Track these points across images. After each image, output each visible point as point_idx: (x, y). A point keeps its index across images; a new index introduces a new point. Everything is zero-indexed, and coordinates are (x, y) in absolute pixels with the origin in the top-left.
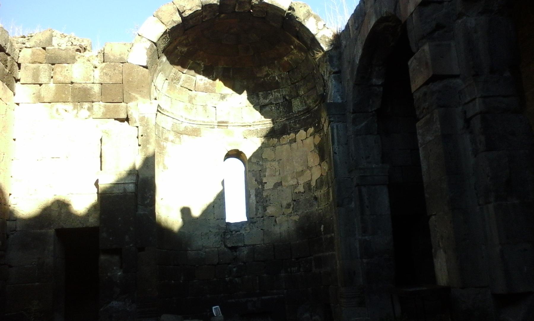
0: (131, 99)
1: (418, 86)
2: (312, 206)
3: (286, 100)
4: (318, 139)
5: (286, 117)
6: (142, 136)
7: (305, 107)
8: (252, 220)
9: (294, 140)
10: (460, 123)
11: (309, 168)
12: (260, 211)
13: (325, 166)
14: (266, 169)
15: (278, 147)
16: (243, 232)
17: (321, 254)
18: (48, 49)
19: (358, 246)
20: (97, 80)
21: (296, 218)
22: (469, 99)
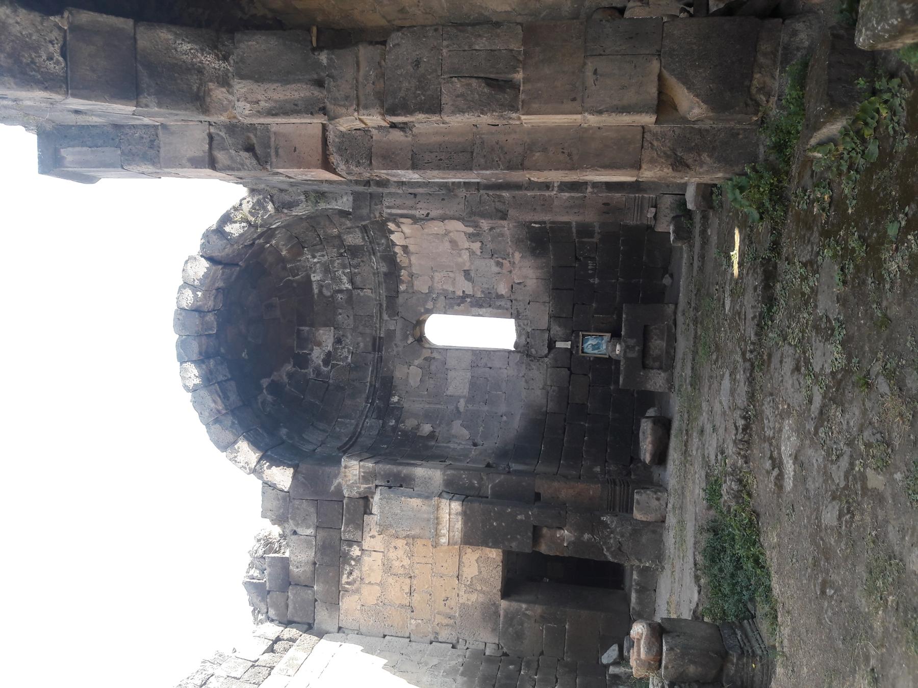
2: (502, 235)
9: (405, 248)
10: (397, 135)
11: (447, 233)
12: (503, 303)
14: (443, 290)
15: (414, 270)
19: (567, 194)
20: (310, 531)
21: (517, 255)
22: (358, 122)
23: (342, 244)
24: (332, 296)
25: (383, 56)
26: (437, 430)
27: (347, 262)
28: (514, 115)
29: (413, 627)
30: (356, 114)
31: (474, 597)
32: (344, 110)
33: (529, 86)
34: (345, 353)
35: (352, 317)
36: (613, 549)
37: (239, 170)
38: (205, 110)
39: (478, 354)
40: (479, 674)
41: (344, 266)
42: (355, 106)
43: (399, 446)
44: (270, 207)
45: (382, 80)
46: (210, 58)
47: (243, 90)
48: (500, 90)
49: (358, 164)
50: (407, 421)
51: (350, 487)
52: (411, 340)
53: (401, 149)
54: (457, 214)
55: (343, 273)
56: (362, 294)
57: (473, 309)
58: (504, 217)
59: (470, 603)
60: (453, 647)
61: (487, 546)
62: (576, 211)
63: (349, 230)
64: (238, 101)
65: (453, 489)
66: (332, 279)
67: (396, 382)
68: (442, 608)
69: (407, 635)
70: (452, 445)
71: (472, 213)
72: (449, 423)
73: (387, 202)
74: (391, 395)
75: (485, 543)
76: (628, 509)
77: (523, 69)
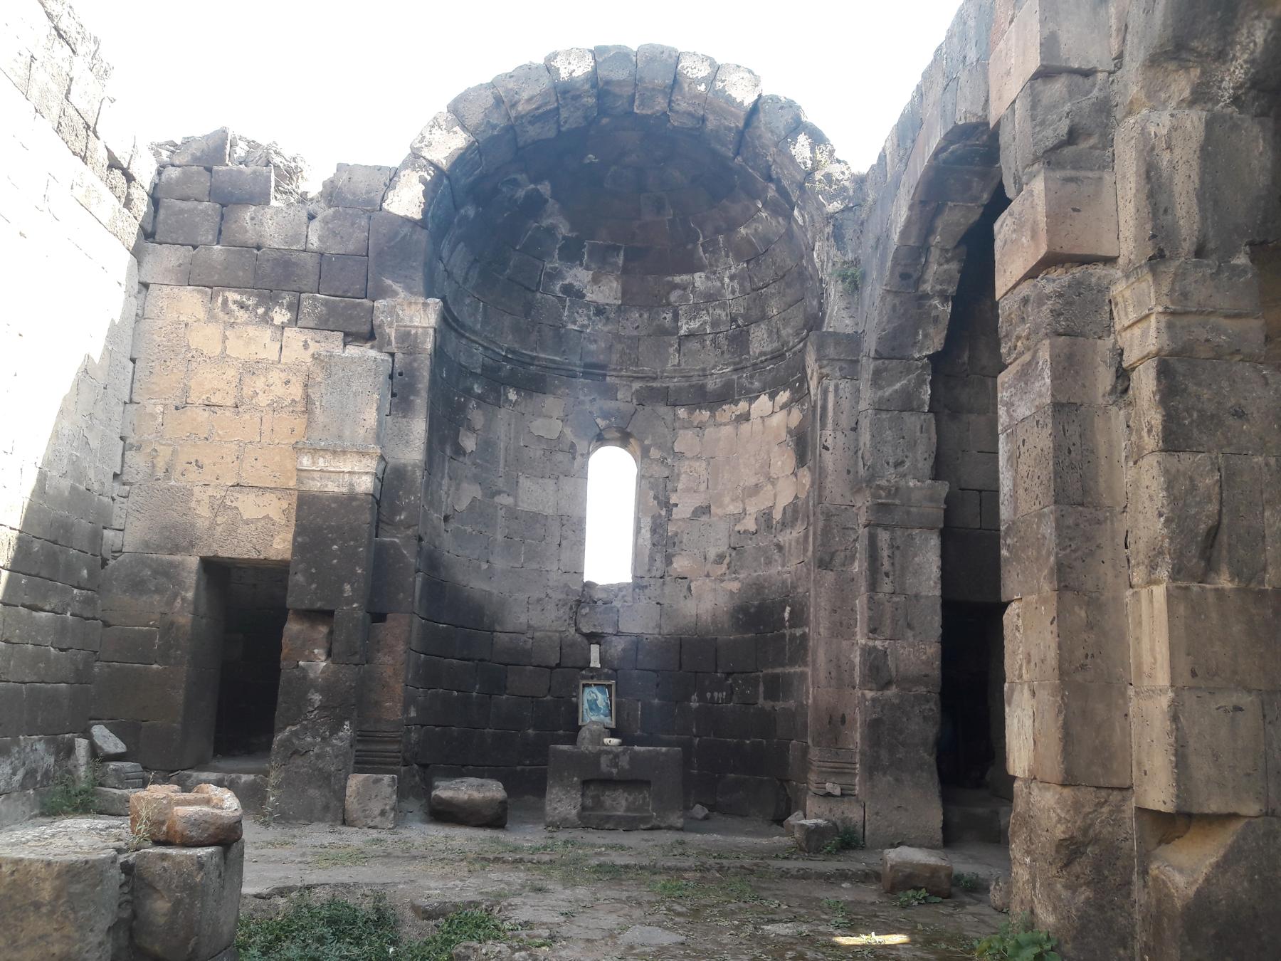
0: (382, 292)
1: (1010, 285)
2: (769, 562)
3: (738, 326)
4: (796, 416)
5: (734, 364)
6: (401, 374)
7: (775, 345)
8: (639, 581)
9: (746, 417)
10: (1105, 379)
11: (772, 481)
13: (806, 477)
14: (679, 475)
15: (709, 431)
16: (617, 603)
17: (778, 670)
18: (218, 172)
21: (735, 586)
22: (1133, 317)
23: (750, 322)
24: (669, 304)
25: (1250, 358)
26: (467, 460)
27: (723, 328)
28: (1163, 573)
29: (149, 409)
30: (1160, 309)
31: (204, 511)
32: (1165, 289)
33: (1211, 598)
34: (581, 320)
35: (635, 333)
36: (296, 741)
37: (1033, 118)
38: (1154, 61)
39: (577, 526)
40: (74, 518)
41: (715, 324)
42: (1172, 307)
43: (458, 391)
44: (835, 206)
45: (1211, 354)
46: (1240, 74)
47: (1188, 124)
48: (1201, 548)
49: (1056, 314)
50: (480, 412)
51: (391, 311)
52: (602, 423)
53: (1084, 386)
54: (827, 492)
55: (705, 322)
56: (671, 350)
57: (649, 520)
58: (824, 564)
59: (193, 504)
60: (116, 476)
61: (296, 534)
62: (833, 674)
63: (774, 333)
64: (1172, 116)
65: (391, 480)
66: (696, 304)
67: (538, 398)
68: (183, 458)
69: (136, 399)
70: (445, 481)
71: (828, 516)
72: (477, 480)
73: (845, 385)
74: (518, 389)
75: (300, 530)
76: (362, 765)
77: (1238, 590)
